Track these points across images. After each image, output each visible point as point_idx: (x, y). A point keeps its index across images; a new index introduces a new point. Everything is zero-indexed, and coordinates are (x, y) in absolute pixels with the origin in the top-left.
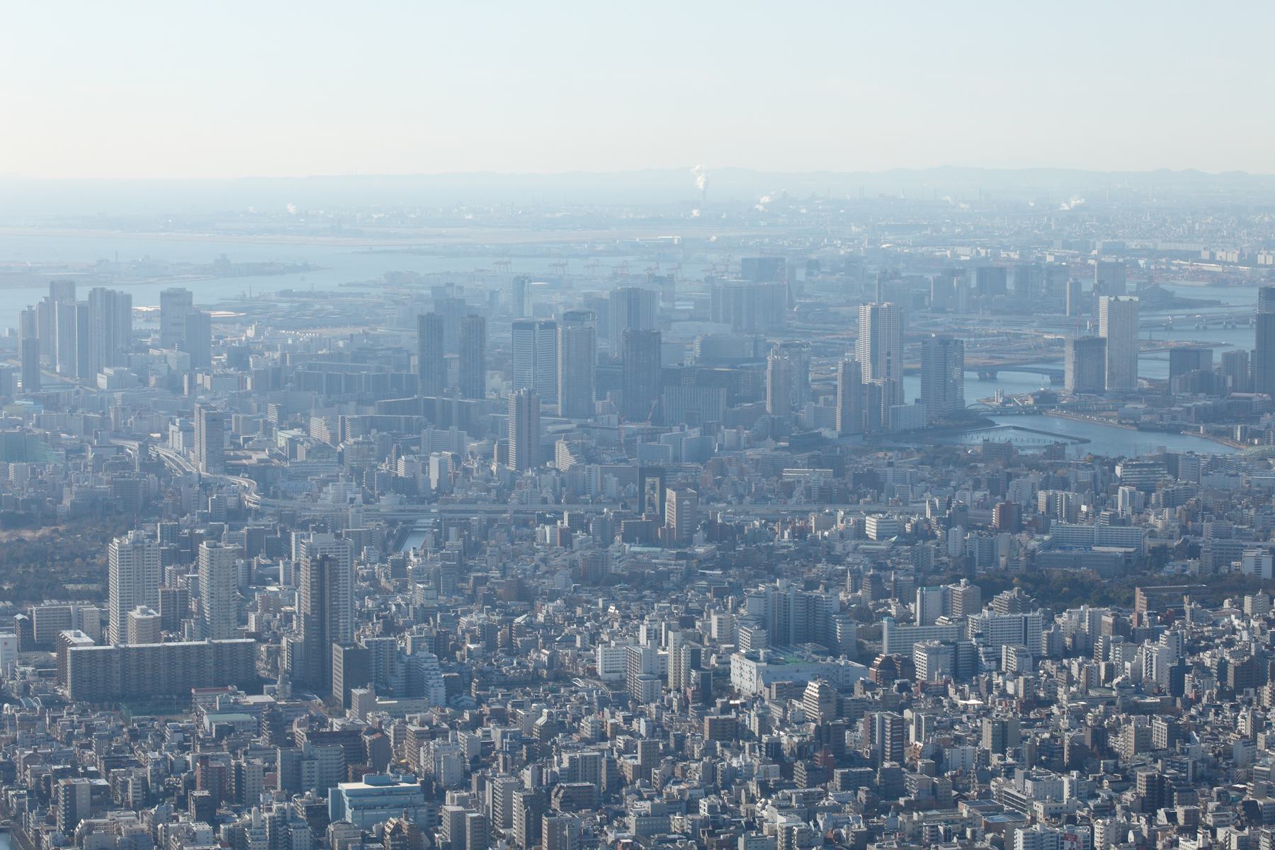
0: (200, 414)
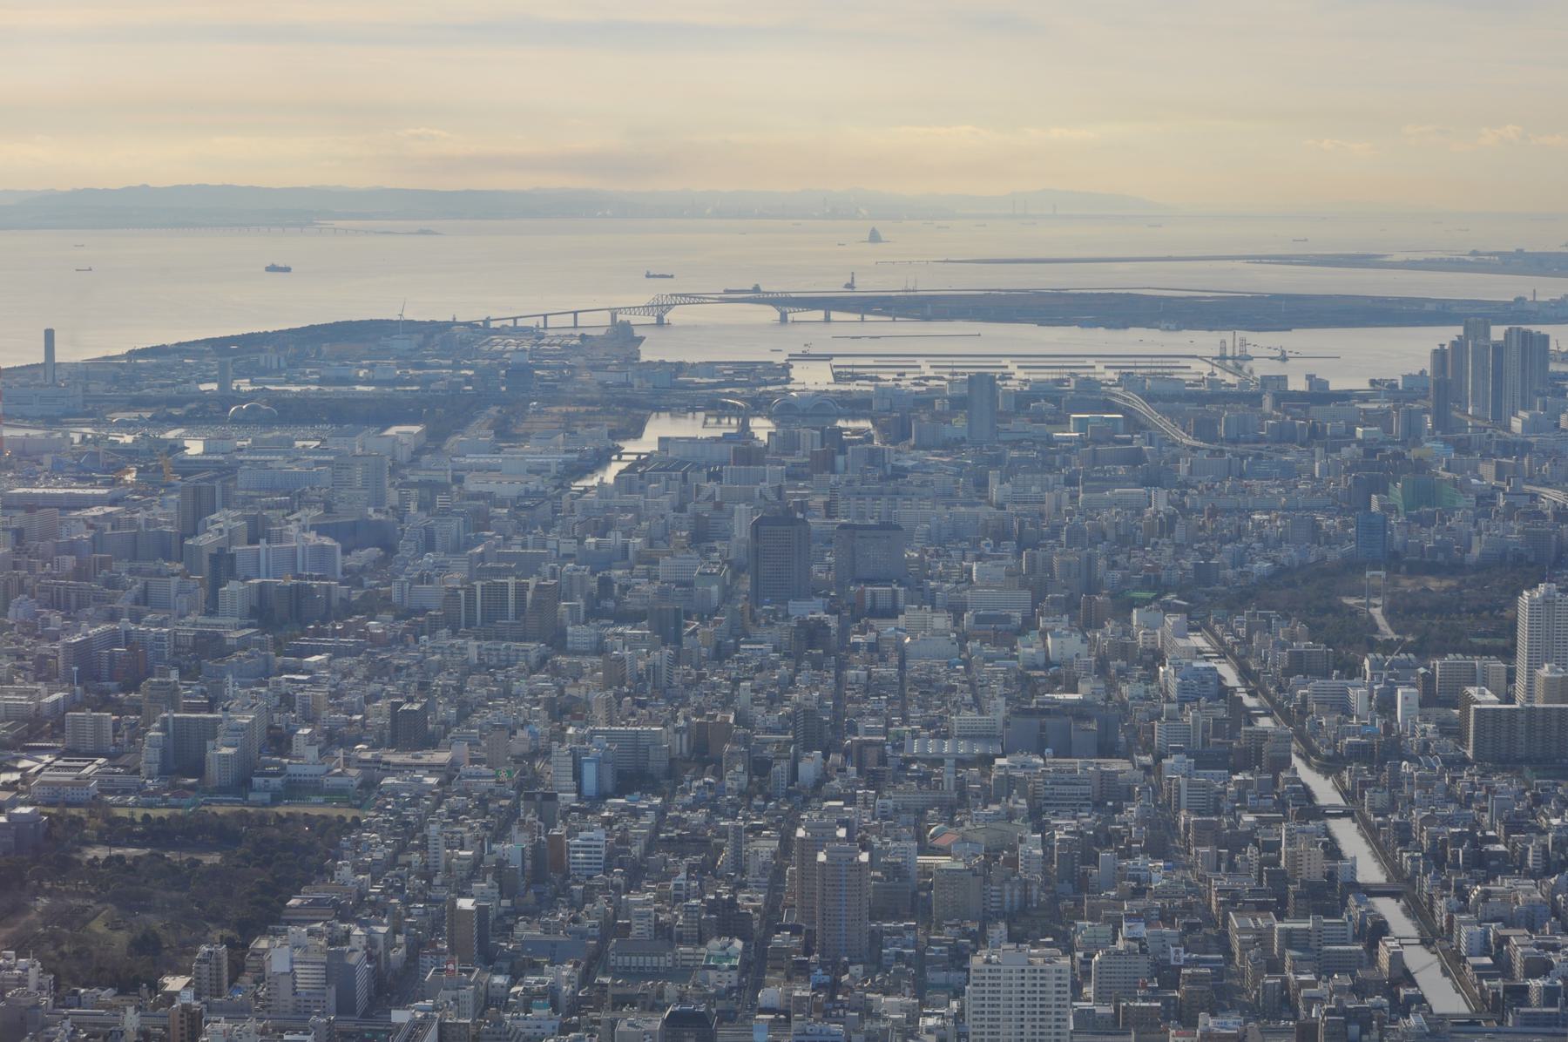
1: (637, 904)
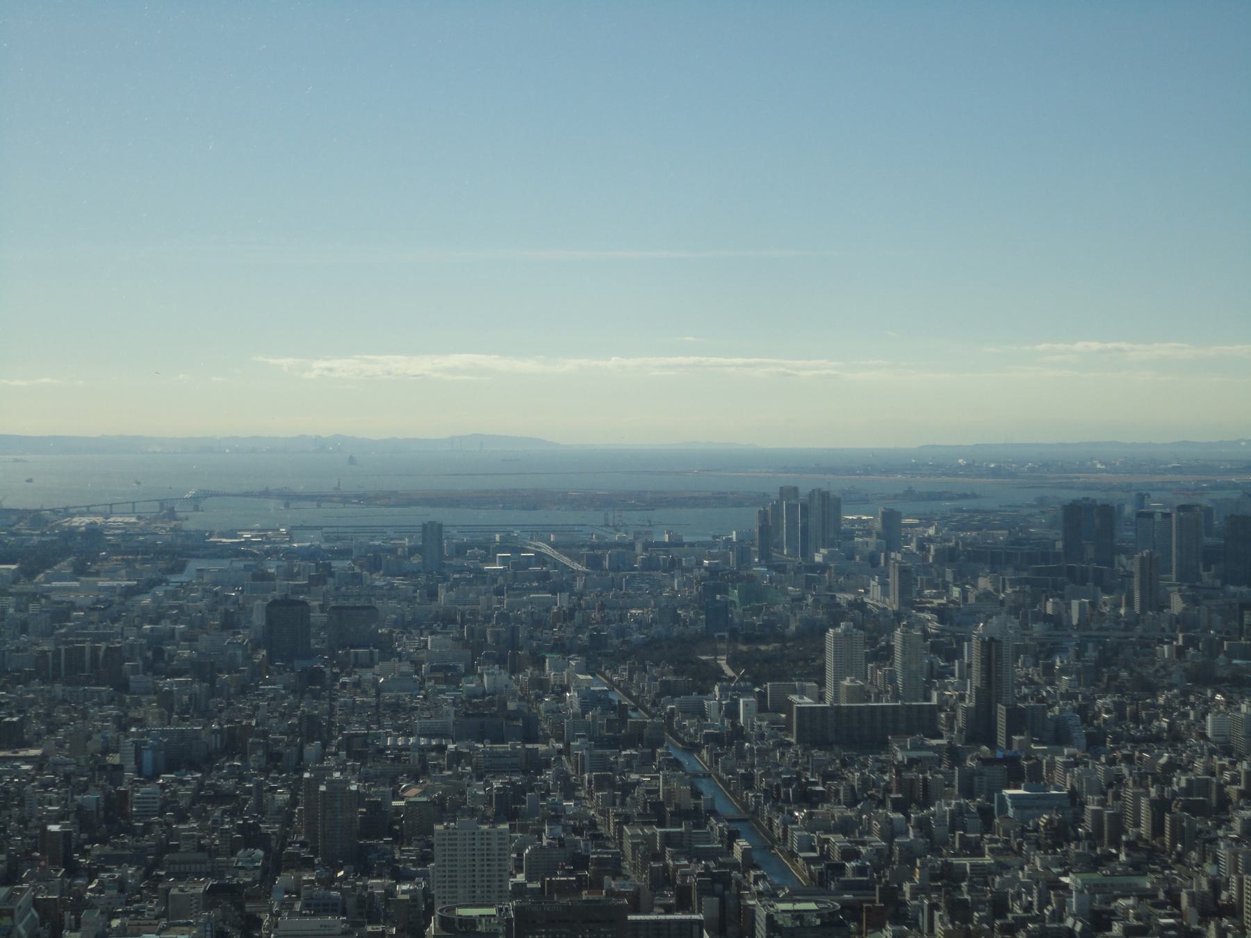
0: (894, 567)
1: (184, 830)
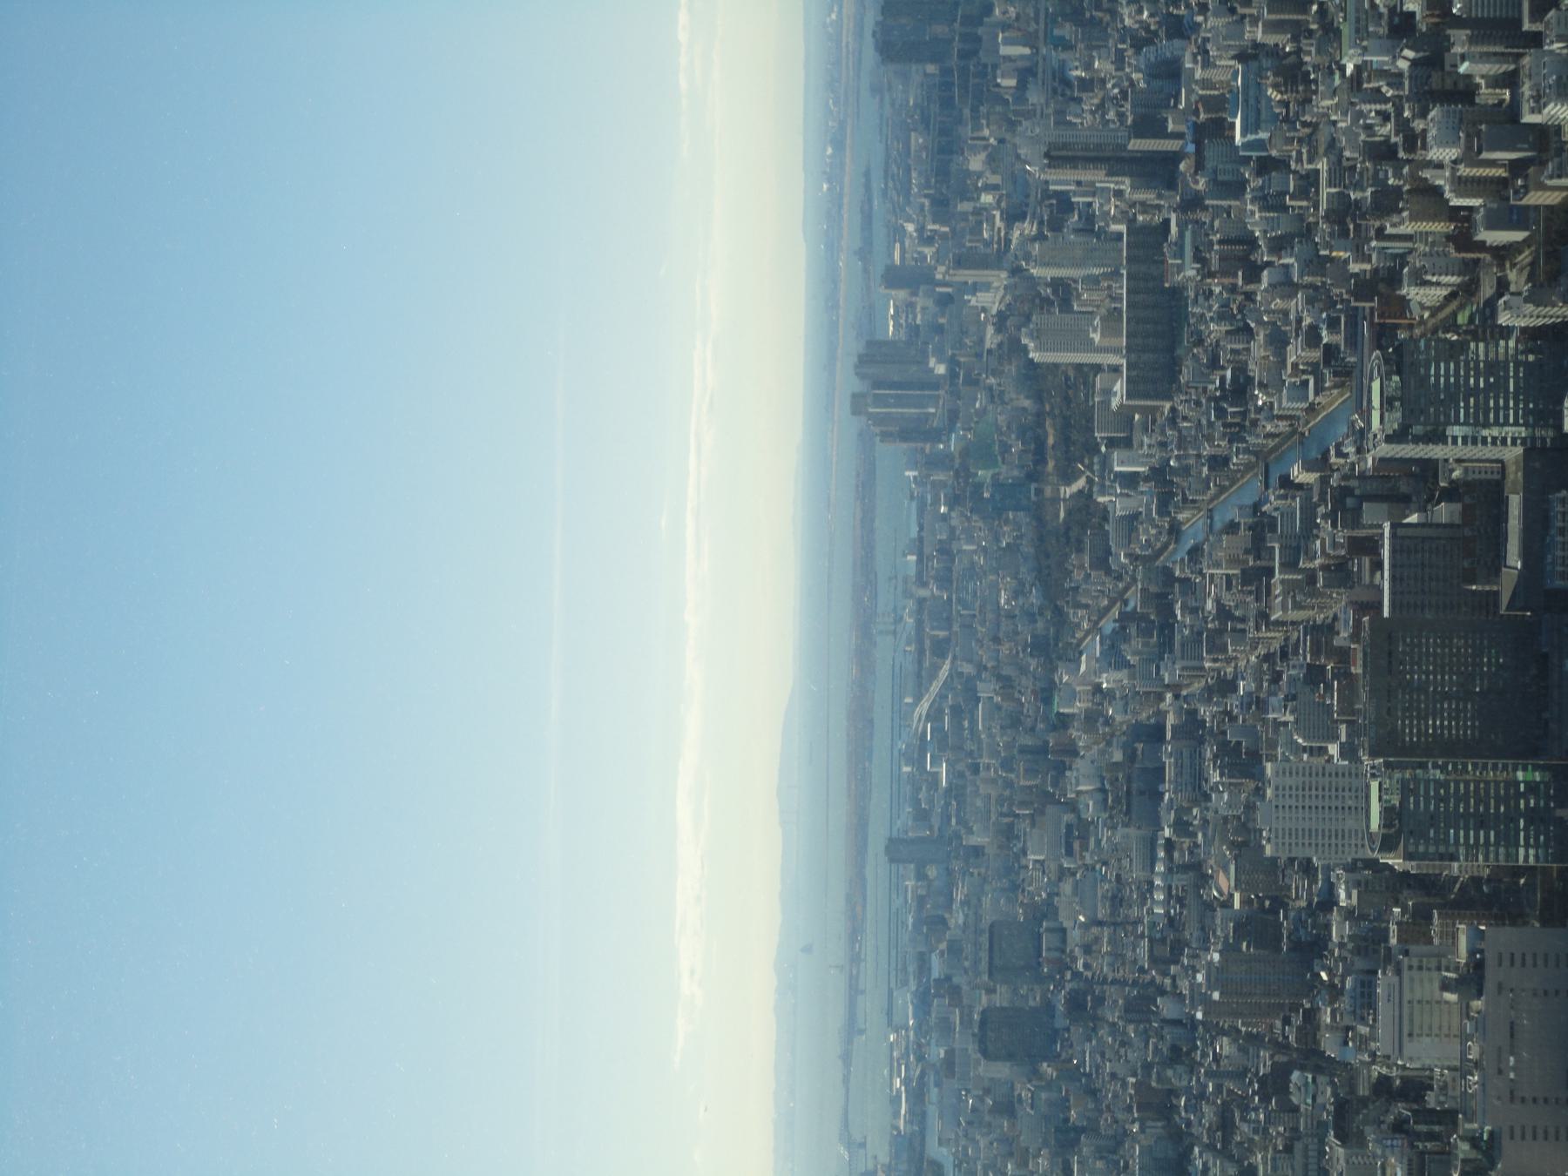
0: (955, 275)
